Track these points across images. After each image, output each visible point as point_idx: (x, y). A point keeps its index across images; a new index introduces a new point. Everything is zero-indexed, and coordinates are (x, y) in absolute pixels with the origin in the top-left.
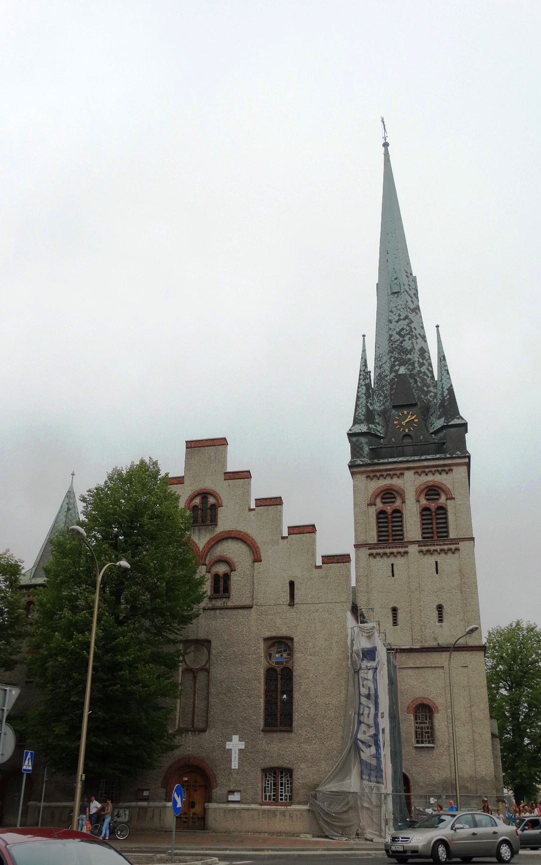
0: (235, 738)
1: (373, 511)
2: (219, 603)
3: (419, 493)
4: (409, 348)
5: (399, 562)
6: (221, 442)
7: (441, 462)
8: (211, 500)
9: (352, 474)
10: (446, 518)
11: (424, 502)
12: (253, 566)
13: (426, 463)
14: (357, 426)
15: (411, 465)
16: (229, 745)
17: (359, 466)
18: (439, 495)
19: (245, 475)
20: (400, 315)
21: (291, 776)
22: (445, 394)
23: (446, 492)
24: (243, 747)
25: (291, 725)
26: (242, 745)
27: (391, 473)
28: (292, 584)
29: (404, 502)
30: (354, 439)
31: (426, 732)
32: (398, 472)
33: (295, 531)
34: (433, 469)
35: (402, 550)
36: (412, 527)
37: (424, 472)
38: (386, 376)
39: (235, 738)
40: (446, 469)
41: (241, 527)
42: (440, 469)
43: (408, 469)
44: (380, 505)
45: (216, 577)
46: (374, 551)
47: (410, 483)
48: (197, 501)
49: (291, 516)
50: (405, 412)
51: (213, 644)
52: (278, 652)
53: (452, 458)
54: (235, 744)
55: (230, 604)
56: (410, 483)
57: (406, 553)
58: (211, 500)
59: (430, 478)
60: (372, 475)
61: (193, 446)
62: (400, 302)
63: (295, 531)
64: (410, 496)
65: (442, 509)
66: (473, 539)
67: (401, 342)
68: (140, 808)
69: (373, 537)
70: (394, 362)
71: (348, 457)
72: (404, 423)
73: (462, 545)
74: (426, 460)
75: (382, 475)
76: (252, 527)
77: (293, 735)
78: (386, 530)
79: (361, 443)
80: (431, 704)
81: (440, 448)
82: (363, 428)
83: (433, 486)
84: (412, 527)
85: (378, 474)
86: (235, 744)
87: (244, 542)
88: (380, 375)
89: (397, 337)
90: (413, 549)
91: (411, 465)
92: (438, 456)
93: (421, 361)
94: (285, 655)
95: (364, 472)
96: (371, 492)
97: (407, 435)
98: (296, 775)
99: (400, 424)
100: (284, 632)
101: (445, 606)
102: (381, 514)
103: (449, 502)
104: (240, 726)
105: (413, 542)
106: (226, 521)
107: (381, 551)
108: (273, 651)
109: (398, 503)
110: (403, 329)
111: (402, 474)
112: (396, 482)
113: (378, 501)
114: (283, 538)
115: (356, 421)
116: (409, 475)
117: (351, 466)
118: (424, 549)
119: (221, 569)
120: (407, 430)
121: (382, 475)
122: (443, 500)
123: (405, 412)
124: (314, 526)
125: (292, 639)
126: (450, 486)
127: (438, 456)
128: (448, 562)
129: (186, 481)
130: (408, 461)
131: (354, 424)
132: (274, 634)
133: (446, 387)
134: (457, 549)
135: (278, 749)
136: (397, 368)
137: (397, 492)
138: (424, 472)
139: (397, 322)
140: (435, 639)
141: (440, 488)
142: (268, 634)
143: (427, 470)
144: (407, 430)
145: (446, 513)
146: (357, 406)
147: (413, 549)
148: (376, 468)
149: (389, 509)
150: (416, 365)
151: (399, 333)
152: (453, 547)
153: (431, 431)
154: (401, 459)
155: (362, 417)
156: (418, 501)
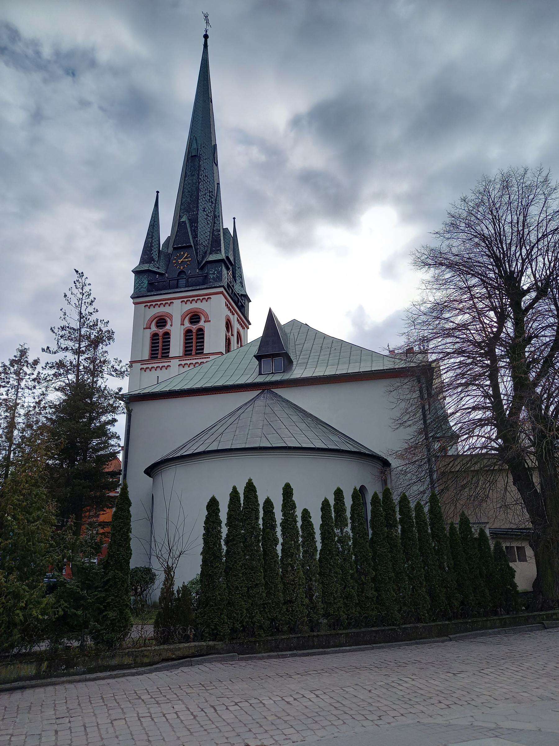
1: (148, 334)
9: (135, 303)
11: (187, 324)
23: (206, 316)
29: (171, 325)
35: (166, 364)
36: (177, 346)
44: (154, 328)
46: (145, 366)
56: (177, 310)
64: (177, 319)
65: (201, 332)
72: (180, 261)
82: (146, 267)
84: (177, 346)
90: (175, 363)
96: (148, 317)
99: (177, 262)
102: (155, 336)
116: (177, 302)
122: (202, 323)
123: (182, 253)
149: (161, 331)
156: (182, 324)
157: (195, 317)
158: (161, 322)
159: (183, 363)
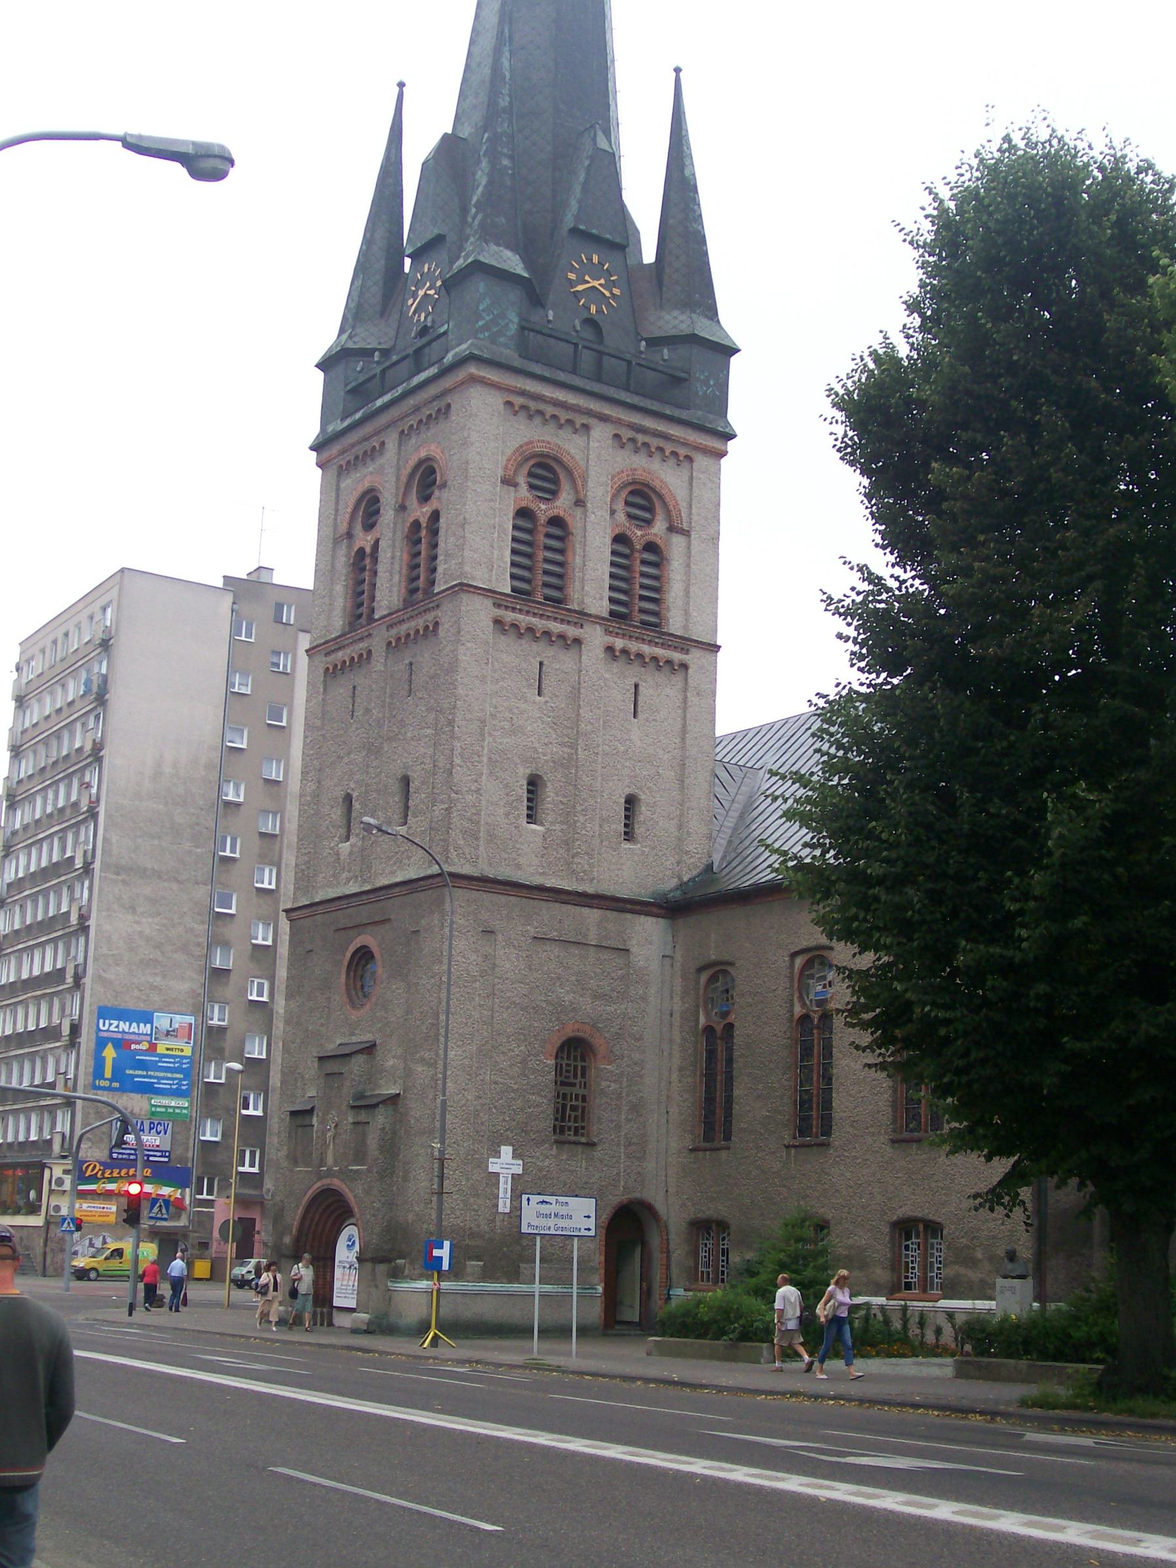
0: (506, 1151)
5: (561, 662)
29: (580, 503)
31: (574, 1108)
32: (579, 420)
39: (506, 1151)
43: (603, 418)
50: (595, 259)
57: (578, 641)
60: (519, 401)
66: (716, 648)
73: (694, 658)
97: (590, 322)
103: (677, 540)
107: (524, 620)
109: (562, 504)
112: (570, 446)
116: (601, 434)
118: (619, 643)
120: (593, 309)
122: (659, 527)
134: (684, 666)
137: (570, 473)
141: (661, 497)
144: (593, 309)
147: (595, 638)
149: (544, 511)
152: (676, 656)
157: (642, 499)
159: (619, 643)
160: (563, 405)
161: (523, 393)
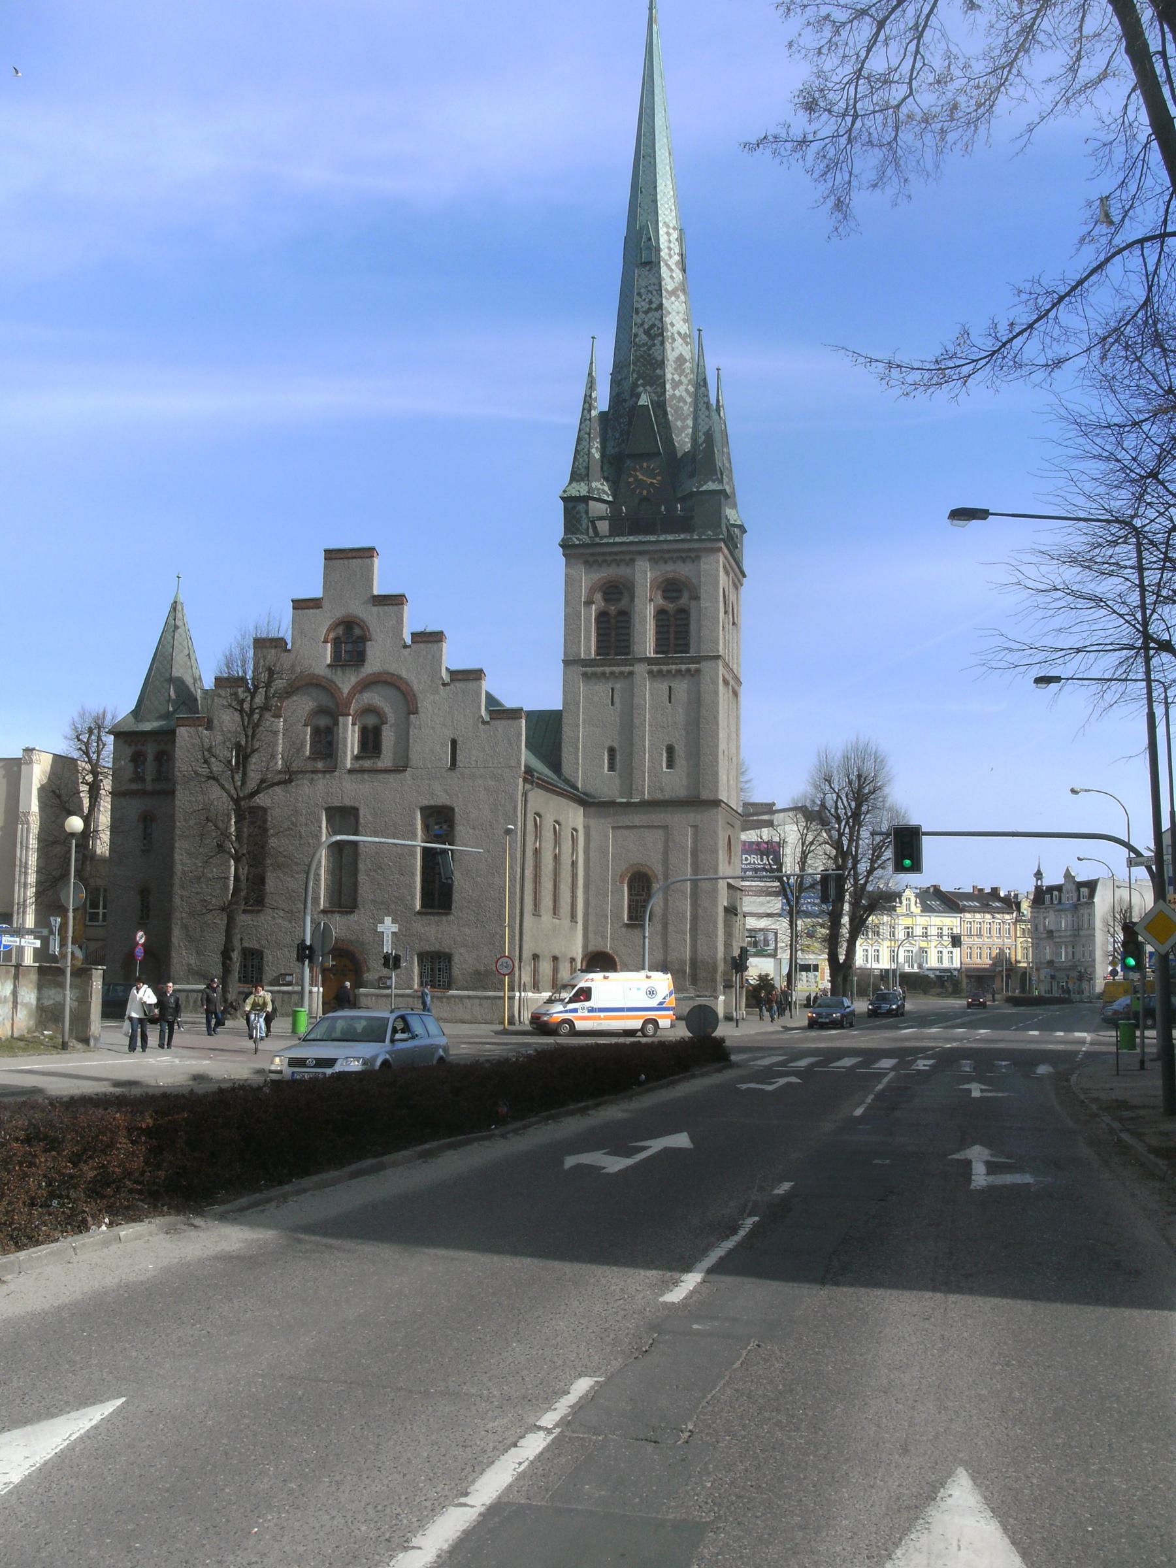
0: (388, 920)
2: (367, 764)
3: (656, 585)
4: (659, 358)
6: (366, 553)
7: (686, 546)
8: (357, 631)
10: (687, 625)
11: (660, 601)
12: (408, 719)
13: (665, 546)
14: (574, 484)
15: (646, 548)
16: (380, 928)
17: (574, 546)
18: (680, 591)
19: (395, 601)
20: (651, 302)
21: (450, 962)
22: (701, 441)
24: (396, 930)
25: (450, 908)
26: (395, 928)
27: (618, 558)
28: (454, 743)
30: (570, 505)
32: (627, 557)
33: (460, 677)
34: (675, 555)
37: (662, 558)
38: (625, 401)
39: (388, 920)
40: (693, 555)
41: (393, 668)
42: (684, 555)
43: (641, 553)
45: (364, 731)
47: (645, 576)
48: (340, 631)
49: (453, 657)
51: (362, 812)
52: (437, 824)
53: (701, 540)
54: (388, 926)
55: (380, 764)
57: (631, 673)
58: (357, 631)
59: (670, 567)
60: (591, 559)
61: (332, 555)
62: (654, 280)
63: (460, 677)
65: (684, 612)
67: (650, 349)
68: (284, 993)
69: (589, 647)
70: (637, 379)
71: (559, 532)
74: (666, 541)
75: (605, 561)
76: (406, 668)
77: (451, 918)
78: (607, 644)
79: (578, 512)
80: (650, 873)
81: (685, 525)
83: (673, 579)
85: (600, 559)
86: (388, 926)
87: (398, 688)
88: (618, 395)
89: (644, 337)
90: (641, 669)
91: (646, 548)
92: (682, 536)
93: (676, 377)
94: (445, 827)
95: (582, 554)
98: (456, 959)
100: (442, 799)
101: (676, 747)
102: (602, 616)
103: (693, 603)
104: (393, 906)
105: (641, 660)
106: (377, 659)
108: (432, 821)
109: (624, 603)
110: (653, 326)
111: (632, 561)
113: (598, 597)
114: (444, 685)
115: (575, 477)
117: (565, 545)
118: (655, 668)
119: (371, 721)
120: (645, 492)
121: (605, 561)
122: (684, 601)
124: (481, 671)
125: (451, 809)
126: (694, 581)
127: (682, 536)
128: (682, 688)
129: (326, 605)
130: (640, 542)
131: (570, 483)
132: (432, 803)
133: (703, 429)
134: (698, 671)
135: (435, 933)
136: (641, 389)
138: (662, 558)
139: (646, 313)
140: (662, 790)
142: (426, 803)
143: (666, 556)
144: (645, 492)
145: (688, 618)
146: (577, 451)
148: (598, 550)
150: (668, 386)
151: (647, 333)
152: (693, 667)
153: (679, 495)
154: (631, 538)
155: (583, 471)
157: (672, 588)
158: (616, 593)
160: (616, 553)
161: (592, 554)
